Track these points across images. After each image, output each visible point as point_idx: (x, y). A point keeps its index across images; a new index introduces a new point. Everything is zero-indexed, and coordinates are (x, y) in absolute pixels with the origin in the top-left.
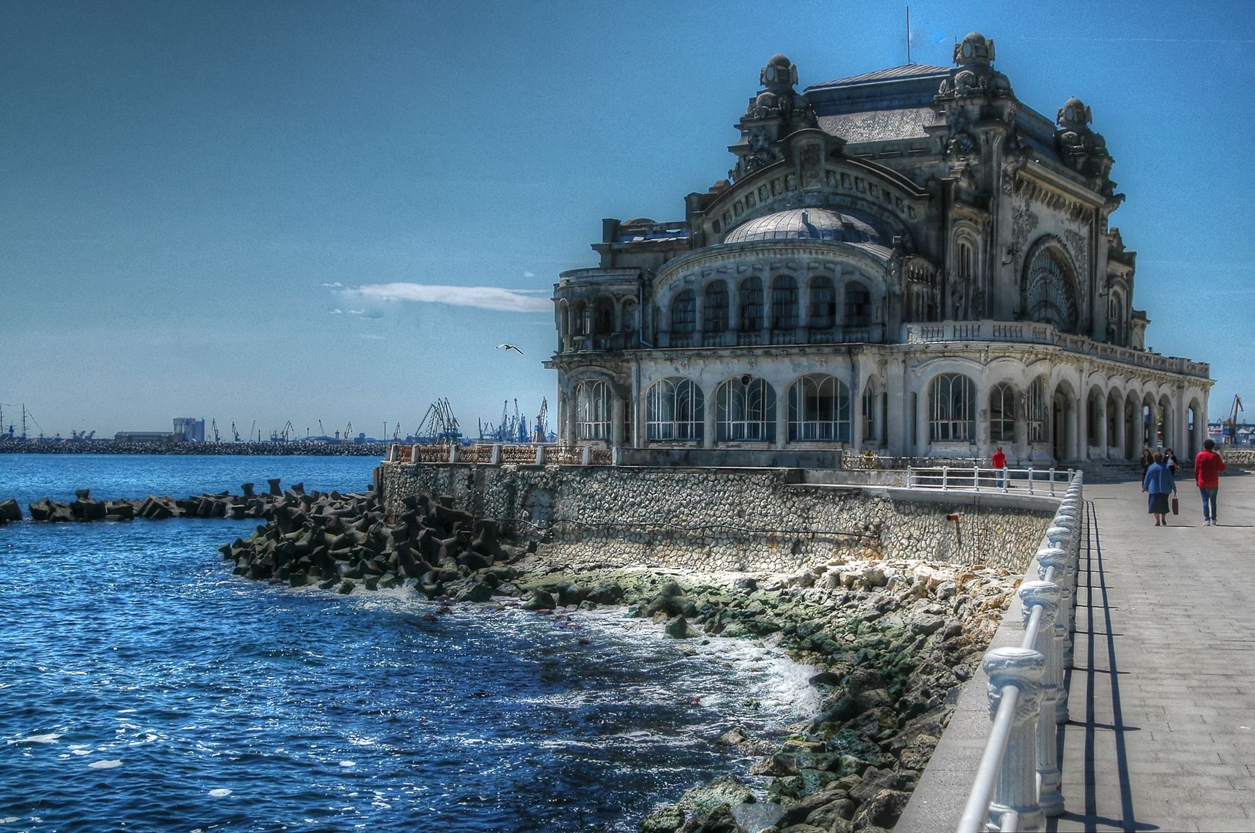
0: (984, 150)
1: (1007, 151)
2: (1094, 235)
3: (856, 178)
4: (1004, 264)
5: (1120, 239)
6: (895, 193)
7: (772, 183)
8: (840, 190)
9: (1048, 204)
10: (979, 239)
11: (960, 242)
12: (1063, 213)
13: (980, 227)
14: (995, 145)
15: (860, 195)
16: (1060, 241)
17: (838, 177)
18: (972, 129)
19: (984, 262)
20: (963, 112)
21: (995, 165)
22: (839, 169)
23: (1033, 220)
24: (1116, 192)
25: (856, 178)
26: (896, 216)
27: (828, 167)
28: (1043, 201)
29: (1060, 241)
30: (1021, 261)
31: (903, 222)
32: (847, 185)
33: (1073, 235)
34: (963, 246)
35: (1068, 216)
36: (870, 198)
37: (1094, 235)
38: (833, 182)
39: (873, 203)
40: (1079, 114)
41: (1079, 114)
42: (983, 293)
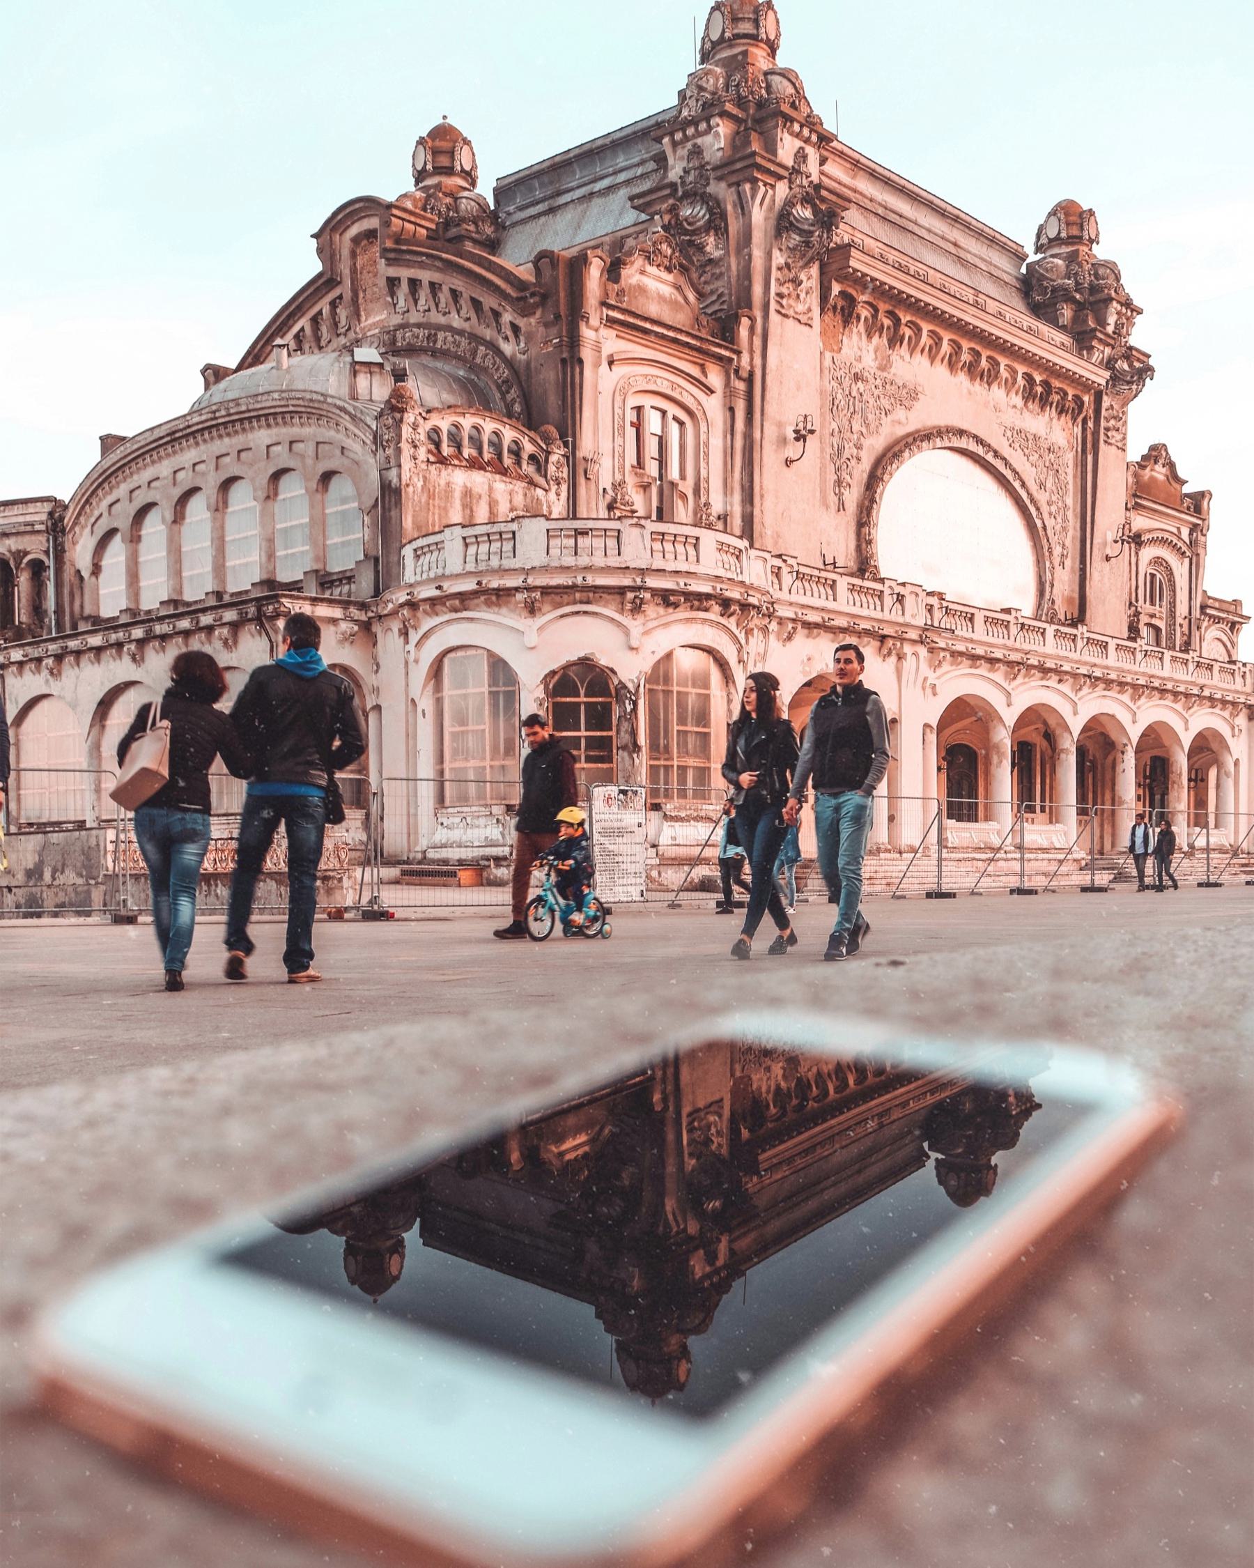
0: (734, 226)
1: (783, 223)
2: (1089, 447)
3: (432, 284)
4: (788, 462)
5: (1171, 465)
6: (489, 301)
7: (315, 321)
8: (414, 318)
9: (952, 366)
10: (713, 406)
12: (998, 392)
14: (758, 216)
15: (442, 320)
16: (979, 441)
17: (405, 285)
19: (729, 453)
20: (697, 152)
21: (758, 254)
22: (405, 273)
25: (432, 284)
26: (498, 352)
27: (392, 272)
30: (861, 470)
31: (509, 363)
32: (422, 302)
35: (1018, 400)
36: (456, 322)
37: (1089, 447)
38: (401, 303)
39: (461, 332)
40: (1072, 225)
41: (1072, 225)
42: (724, 518)
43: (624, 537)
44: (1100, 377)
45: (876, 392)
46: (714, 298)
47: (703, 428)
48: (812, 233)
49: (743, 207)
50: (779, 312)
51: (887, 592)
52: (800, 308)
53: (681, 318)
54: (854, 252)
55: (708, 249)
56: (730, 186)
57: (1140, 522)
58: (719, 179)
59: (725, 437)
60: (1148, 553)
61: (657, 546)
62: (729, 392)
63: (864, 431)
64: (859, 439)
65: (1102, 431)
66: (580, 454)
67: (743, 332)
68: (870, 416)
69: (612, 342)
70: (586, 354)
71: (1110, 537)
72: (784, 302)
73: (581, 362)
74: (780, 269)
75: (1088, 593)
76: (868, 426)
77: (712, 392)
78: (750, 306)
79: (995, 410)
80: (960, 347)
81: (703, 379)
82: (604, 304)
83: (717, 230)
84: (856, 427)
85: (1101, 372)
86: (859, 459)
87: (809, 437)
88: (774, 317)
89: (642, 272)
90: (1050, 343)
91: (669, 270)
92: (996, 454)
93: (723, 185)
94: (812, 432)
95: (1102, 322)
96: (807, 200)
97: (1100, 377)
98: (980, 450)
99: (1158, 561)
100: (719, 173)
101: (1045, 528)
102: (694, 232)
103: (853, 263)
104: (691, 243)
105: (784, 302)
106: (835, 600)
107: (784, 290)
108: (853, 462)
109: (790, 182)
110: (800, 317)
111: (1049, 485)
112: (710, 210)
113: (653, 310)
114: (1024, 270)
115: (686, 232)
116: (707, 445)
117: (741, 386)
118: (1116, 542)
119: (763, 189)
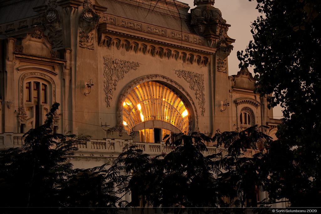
1: (81, 19)
9: (153, 54)
10: (57, 79)
11: (32, 81)
12: (172, 60)
13: (57, 71)
16: (164, 77)
18: (59, 8)
21: (72, 29)
23: (135, 66)
24: (232, 44)
28: (144, 52)
29: (164, 77)
33: (182, 73)
34: (37, 84)
35: (182, 61)
43: (4, 138)
44: (213, 51)
45: (121, 66)
46: (59, 42)
47: (53, 86)
48: (90, 22)
49: (68, 14)
50: (80, 47)
51: (107, 142)
52: (89, 44)
53: (45, 53)
54: (107, 24)
55: (57, 27)
56: (63, 8)
57: (236, 96)
58: (60, 5)
59: (62, 89)
60: (240, 107)
61: (16, 141)
62: (63, 74)
63: (117, 79)
64: (115, 82)
65: (216, 68)
66: (6, 100)
67: (67, 55)
69: (18, 64)
70: (8, 69)
71: (222, 103)
72: (83, 44)
73: (6, 72)
74: (80, 33)
75: (213, 124)
76: (118, 77)
77: (57, 75)
78: (70, 47)
79: (171, 67)
80: (155, 48)
81: (53, 71)
82: (14, 53)
83: (59, 22)
84: (113, 79)
85: (213, 49)
86: (115, 89)
87: (92, 87)
88: (78, 48)
89: (30, 40)
90: (194, 41)
91: (40, 38)
92: (171, 81)
93: (61, 7)
94: (92, 85)
95: (215, 32)
96: (89, 11)
97: (213, 51)
98: (165, 80)
99: (245, 109)
100: (59, 4)
101: (193, 104)
102: (51, 23)
103: (108, 28)
104: (51, 26)
105: (83, 44)
106: (86, 148)
107: (83, 40)
108: (113, 90)
109: (84, 6)
110: (89, 47)
111: (195, 88)
112: (57, 15)
113: (33, 52)
114: (189, 12)
115: (49, 23)
116: (55, 91)
117: (67, 72)
118: (224, 105)
119: (74, 9)
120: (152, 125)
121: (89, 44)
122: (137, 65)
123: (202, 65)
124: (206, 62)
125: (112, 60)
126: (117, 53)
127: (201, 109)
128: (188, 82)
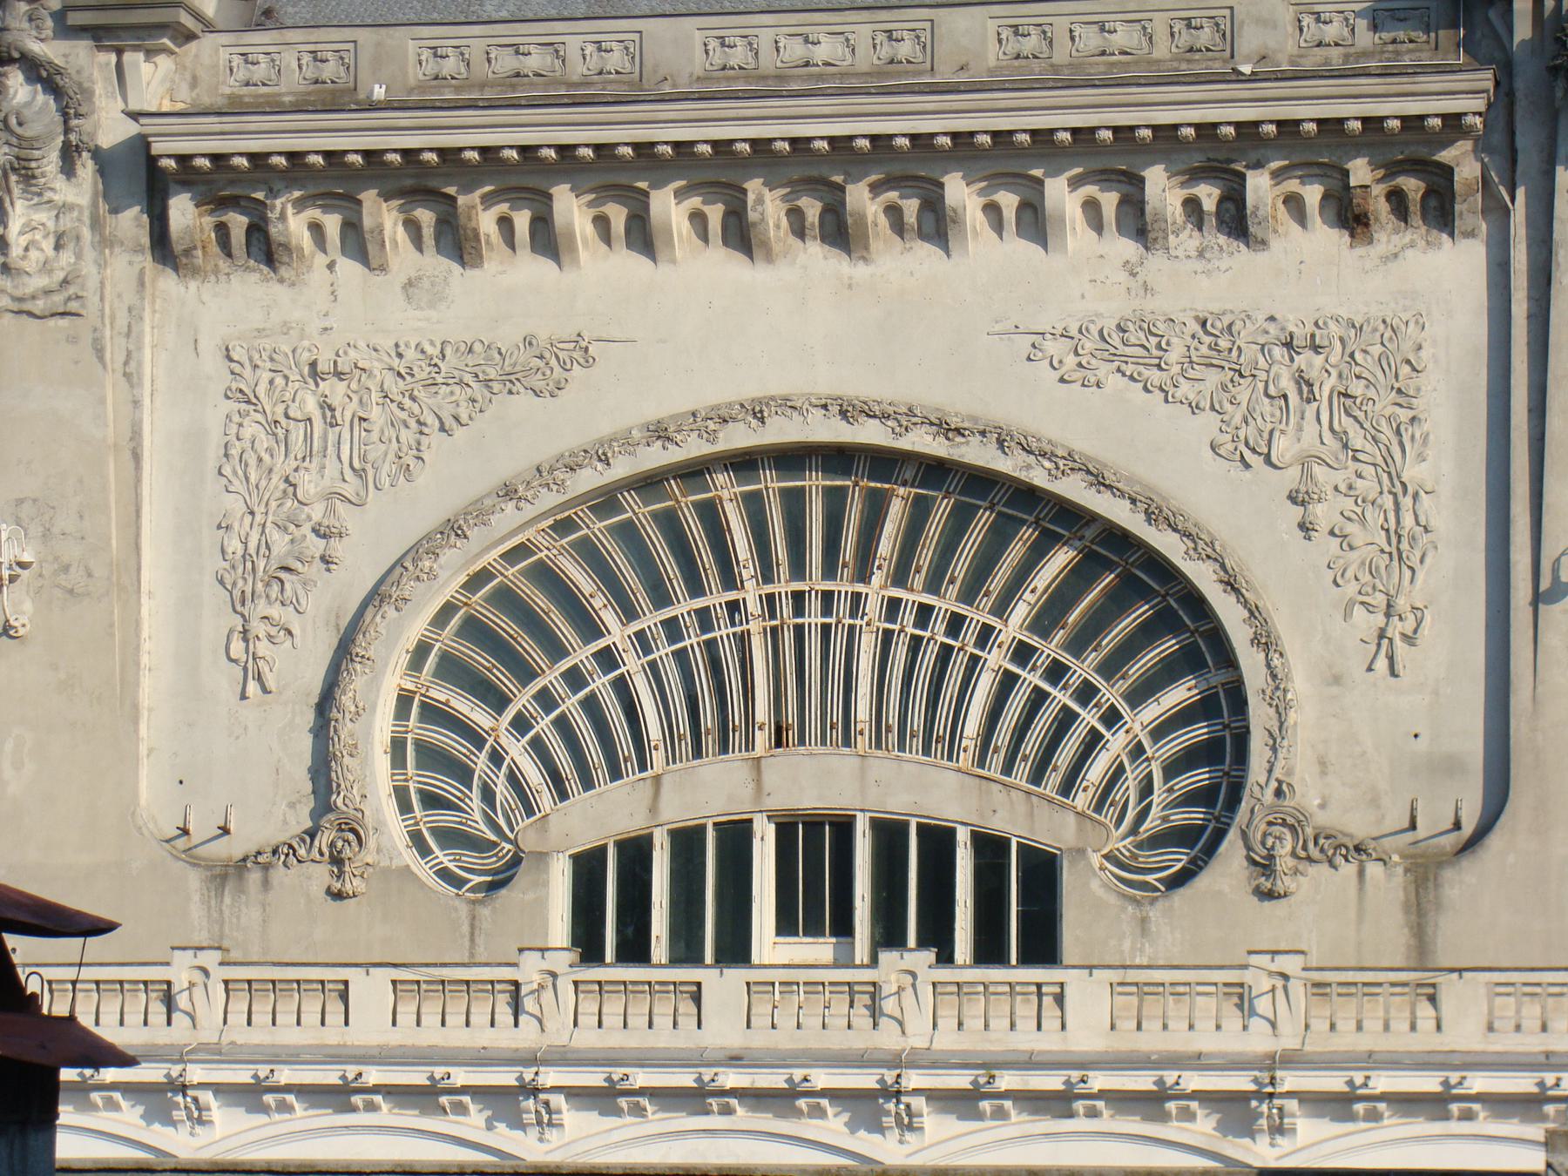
68: (375, 452)
92: (946, 429)
98: (871, 433)
110: (39, 306)
120: (748, 791)
121: (38, 282)
122: (581, 351)
123: (1408, 236)
124: (1440, 210)
125: (306, 357)
126: (359, 300)
127: (1366, 623)
128: (1195, 408)
